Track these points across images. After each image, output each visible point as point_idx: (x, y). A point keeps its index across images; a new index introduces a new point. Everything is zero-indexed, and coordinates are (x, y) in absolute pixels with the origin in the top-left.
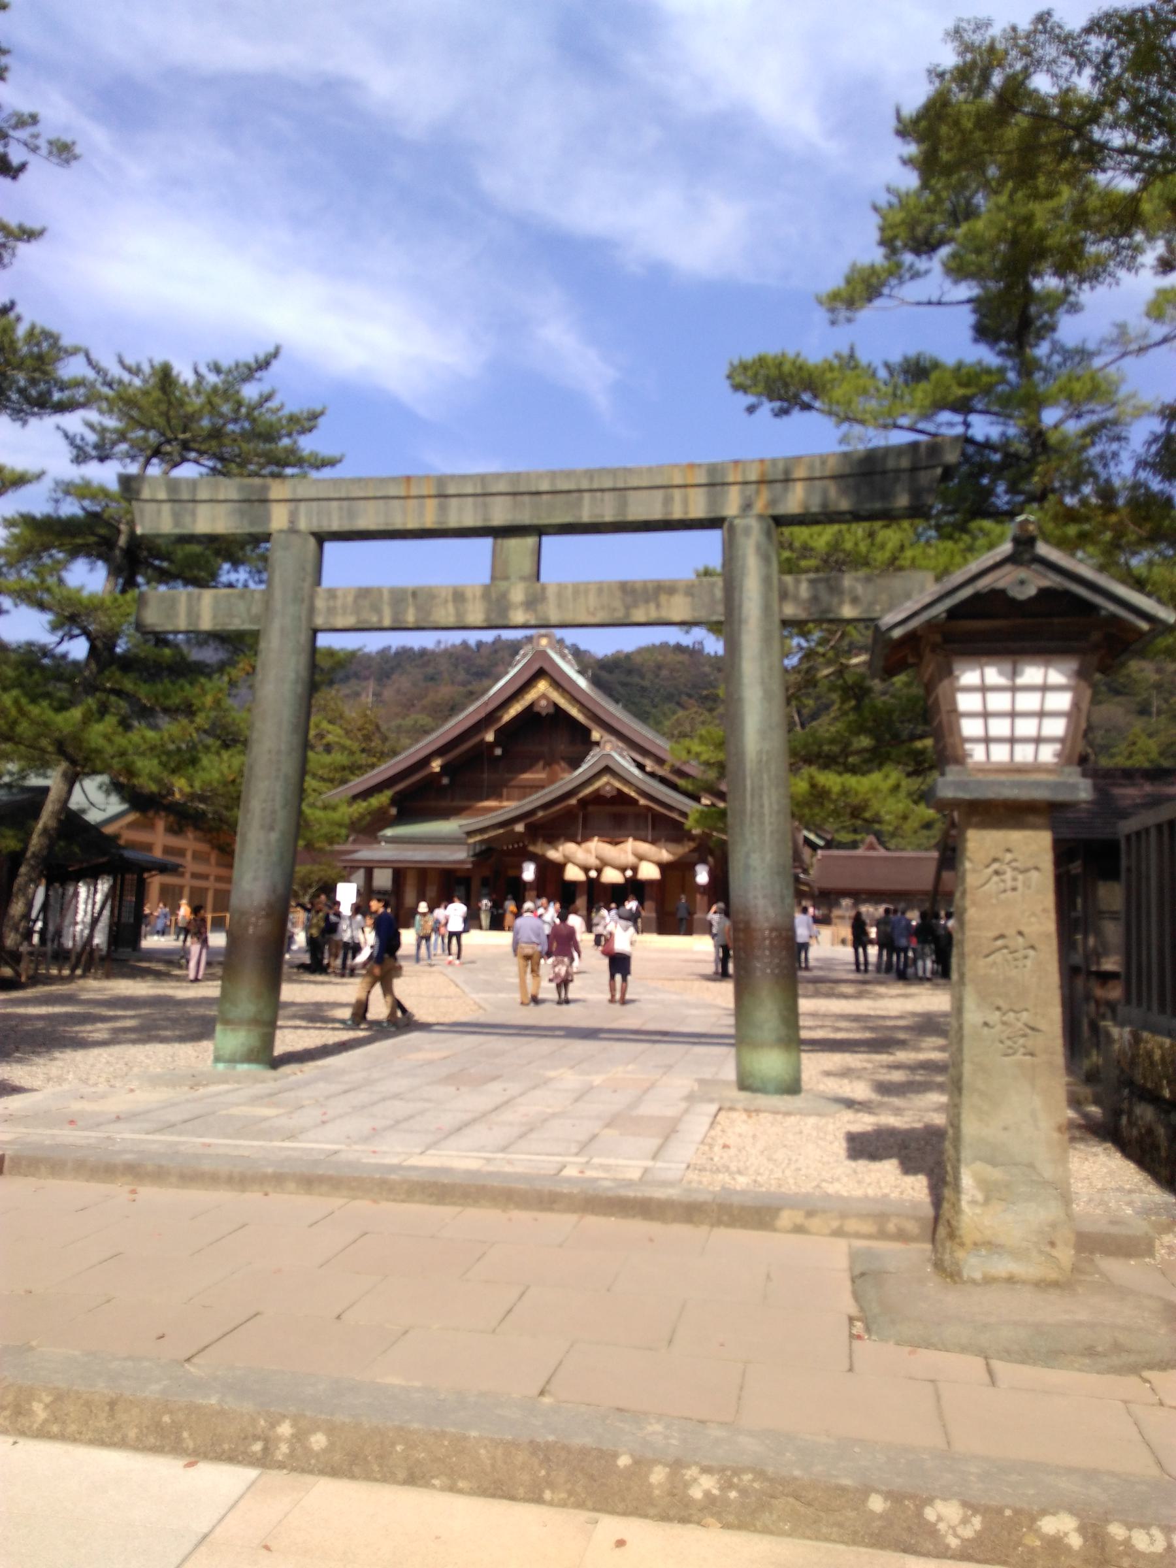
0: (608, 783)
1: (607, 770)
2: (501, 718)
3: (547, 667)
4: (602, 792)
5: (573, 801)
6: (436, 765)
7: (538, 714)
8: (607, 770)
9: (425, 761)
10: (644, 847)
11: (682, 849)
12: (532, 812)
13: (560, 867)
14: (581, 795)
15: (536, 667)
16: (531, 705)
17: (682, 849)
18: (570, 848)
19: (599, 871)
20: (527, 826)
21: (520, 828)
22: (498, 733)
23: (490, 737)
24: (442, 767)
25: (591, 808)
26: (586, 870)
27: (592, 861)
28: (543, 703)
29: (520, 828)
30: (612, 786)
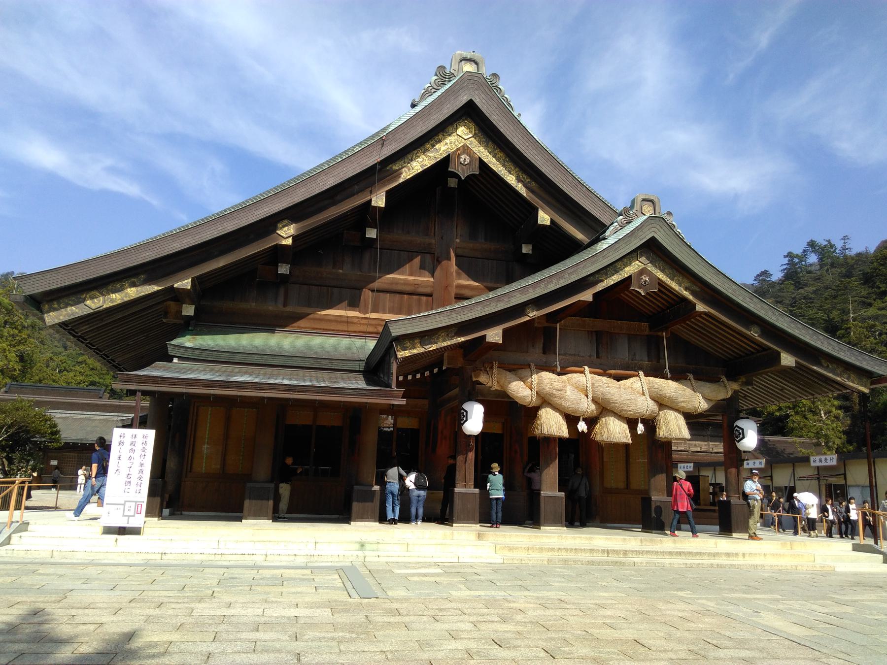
0: (642, 272)
2: (398, 174)
5: (587, 296)
6: (287, 234)
9: (269, 225)
10: (670, 388)
11: (724, 391)
12: (518, 310)
13: (532, 413)
14: (600, 287)
16: (446, 160)
17: (724, 391)
18: (547, 380)
19: (592, 422)
20: (505, 332)
22: (389, 194)
24: (295, 238)
26: (571, 420)
27: (587, 406)
28: (465, 158)
30: (650, 274)
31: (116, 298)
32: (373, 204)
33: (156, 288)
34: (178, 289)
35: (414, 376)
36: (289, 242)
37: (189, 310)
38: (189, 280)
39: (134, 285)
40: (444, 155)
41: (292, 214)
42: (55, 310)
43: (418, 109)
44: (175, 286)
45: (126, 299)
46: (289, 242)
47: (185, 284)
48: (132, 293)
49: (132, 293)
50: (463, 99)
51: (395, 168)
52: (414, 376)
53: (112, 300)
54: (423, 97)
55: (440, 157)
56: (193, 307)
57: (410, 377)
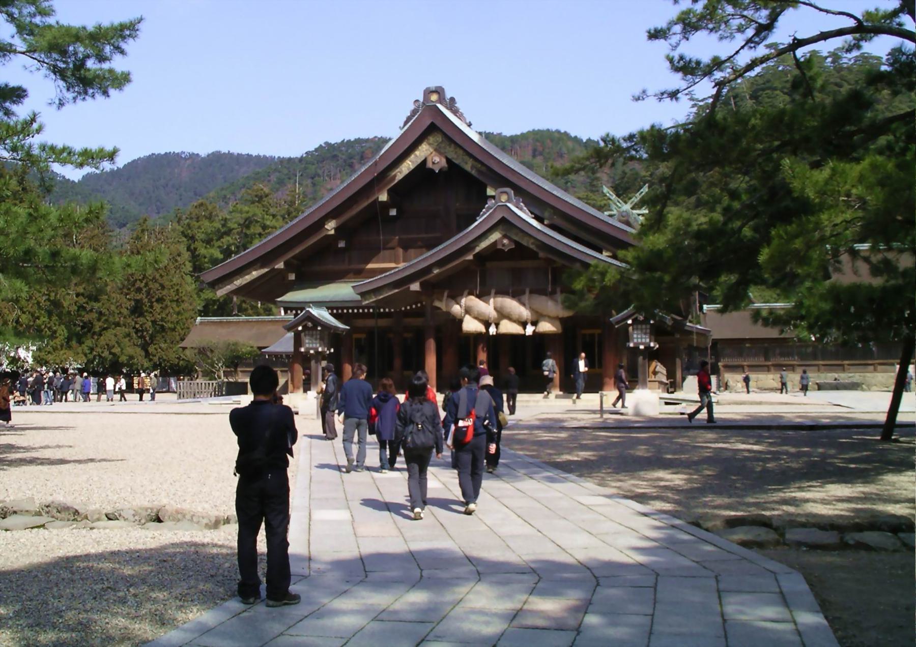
1: (503, 222)
3: (438, 123)
4: (499, 247)
6: (331, 226)
7: (432, 171)
8: (503, 222)
9: (319, 225)
12: (428, 270)
14: (478, 249)
15: (428, 122)
16: (424, 162)
21: (415, 287)
22: (390, 192)
23: (384, 197)
24: (336, 229)
25: (489, 265)
29: (415, 287)
31: (248, 278)
32: (380, 200)
33: (266, 270)
34: (277, 269)
35: (416, 306)
36: (332, 232)
37: (292, 277)
38: (282, 263)
39: (256, 270)
40: (422, 159)
41: (333, 214)
42: (221, 288)
43: (406, 128)
44: (276, 267)
45: (252, 278)
46: (332, 232)
47: (280, 265)
48: (255, 274)
49: (255, 274)
50: (428, 122)
51: (393, 174)
52: (416, 306)
53: (246, 280)
54: (406, 123)
55: (419, 161)
56: (294, 275)
57: (414, 306)
